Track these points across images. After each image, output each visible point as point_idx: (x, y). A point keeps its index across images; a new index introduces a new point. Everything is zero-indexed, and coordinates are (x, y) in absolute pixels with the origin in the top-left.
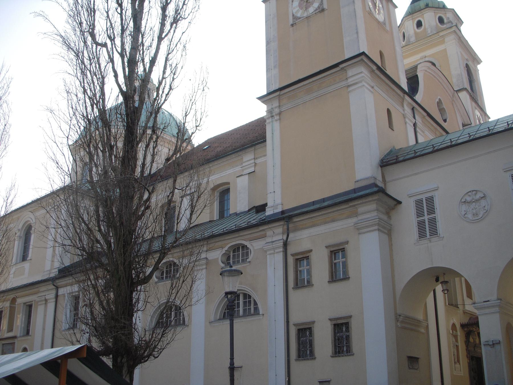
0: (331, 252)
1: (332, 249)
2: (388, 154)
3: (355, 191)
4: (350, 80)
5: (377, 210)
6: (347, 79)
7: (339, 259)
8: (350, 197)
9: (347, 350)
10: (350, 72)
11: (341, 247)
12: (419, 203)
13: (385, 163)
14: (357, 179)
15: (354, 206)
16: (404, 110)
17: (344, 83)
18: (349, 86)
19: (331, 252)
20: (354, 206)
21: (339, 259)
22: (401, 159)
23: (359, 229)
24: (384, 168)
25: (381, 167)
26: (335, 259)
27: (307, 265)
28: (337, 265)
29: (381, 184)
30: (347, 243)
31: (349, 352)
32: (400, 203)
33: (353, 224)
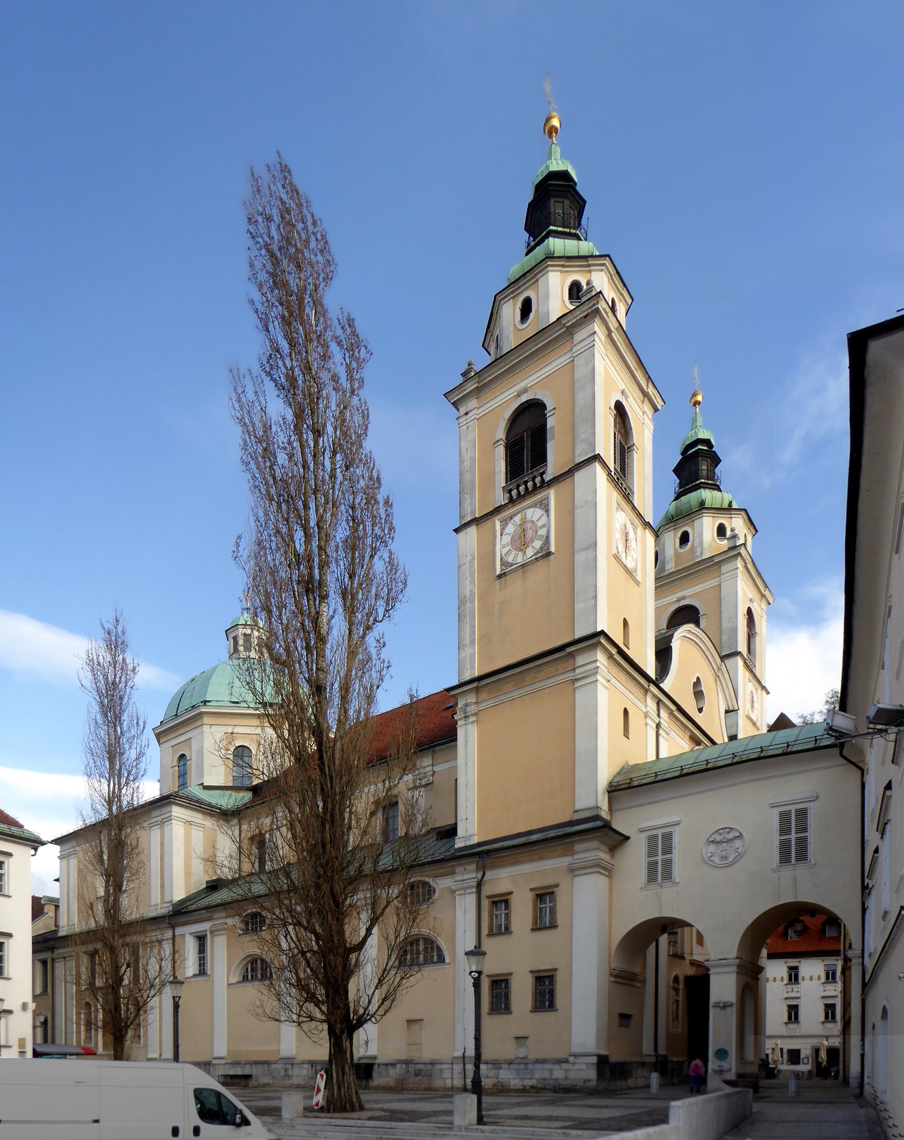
0: (537, 895)
1: (538, 892)
2: (618, 774)
3: (571, 823)
4: (578, 671)
5: (598, 849)
6: (574, 669)
7: (546, 903)
8: (566, 832)
9: (549, 1005)
10: (580, 660)
11: (550, 890)
12: (652, 840)
13: (613, 788)
14: (578, 807)
15: (571, 842)
16: (646, 706)
17: (569, 676)
18: (577, 680)
19: (537, 895)
20: (571, 842)
21: (546, 903)
22: (635, 783)
23: (572, 871)
24: (611, 794)
25: (609, 792)
26: (541, 904)
27: (505, 910)
28: (544, 910)
29: (605, 815)
30: (557, 886)
31: (552, 1006)
32: (627, 838)
33: (566, 864)
